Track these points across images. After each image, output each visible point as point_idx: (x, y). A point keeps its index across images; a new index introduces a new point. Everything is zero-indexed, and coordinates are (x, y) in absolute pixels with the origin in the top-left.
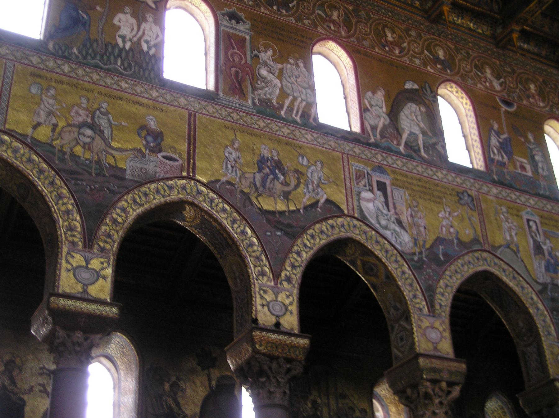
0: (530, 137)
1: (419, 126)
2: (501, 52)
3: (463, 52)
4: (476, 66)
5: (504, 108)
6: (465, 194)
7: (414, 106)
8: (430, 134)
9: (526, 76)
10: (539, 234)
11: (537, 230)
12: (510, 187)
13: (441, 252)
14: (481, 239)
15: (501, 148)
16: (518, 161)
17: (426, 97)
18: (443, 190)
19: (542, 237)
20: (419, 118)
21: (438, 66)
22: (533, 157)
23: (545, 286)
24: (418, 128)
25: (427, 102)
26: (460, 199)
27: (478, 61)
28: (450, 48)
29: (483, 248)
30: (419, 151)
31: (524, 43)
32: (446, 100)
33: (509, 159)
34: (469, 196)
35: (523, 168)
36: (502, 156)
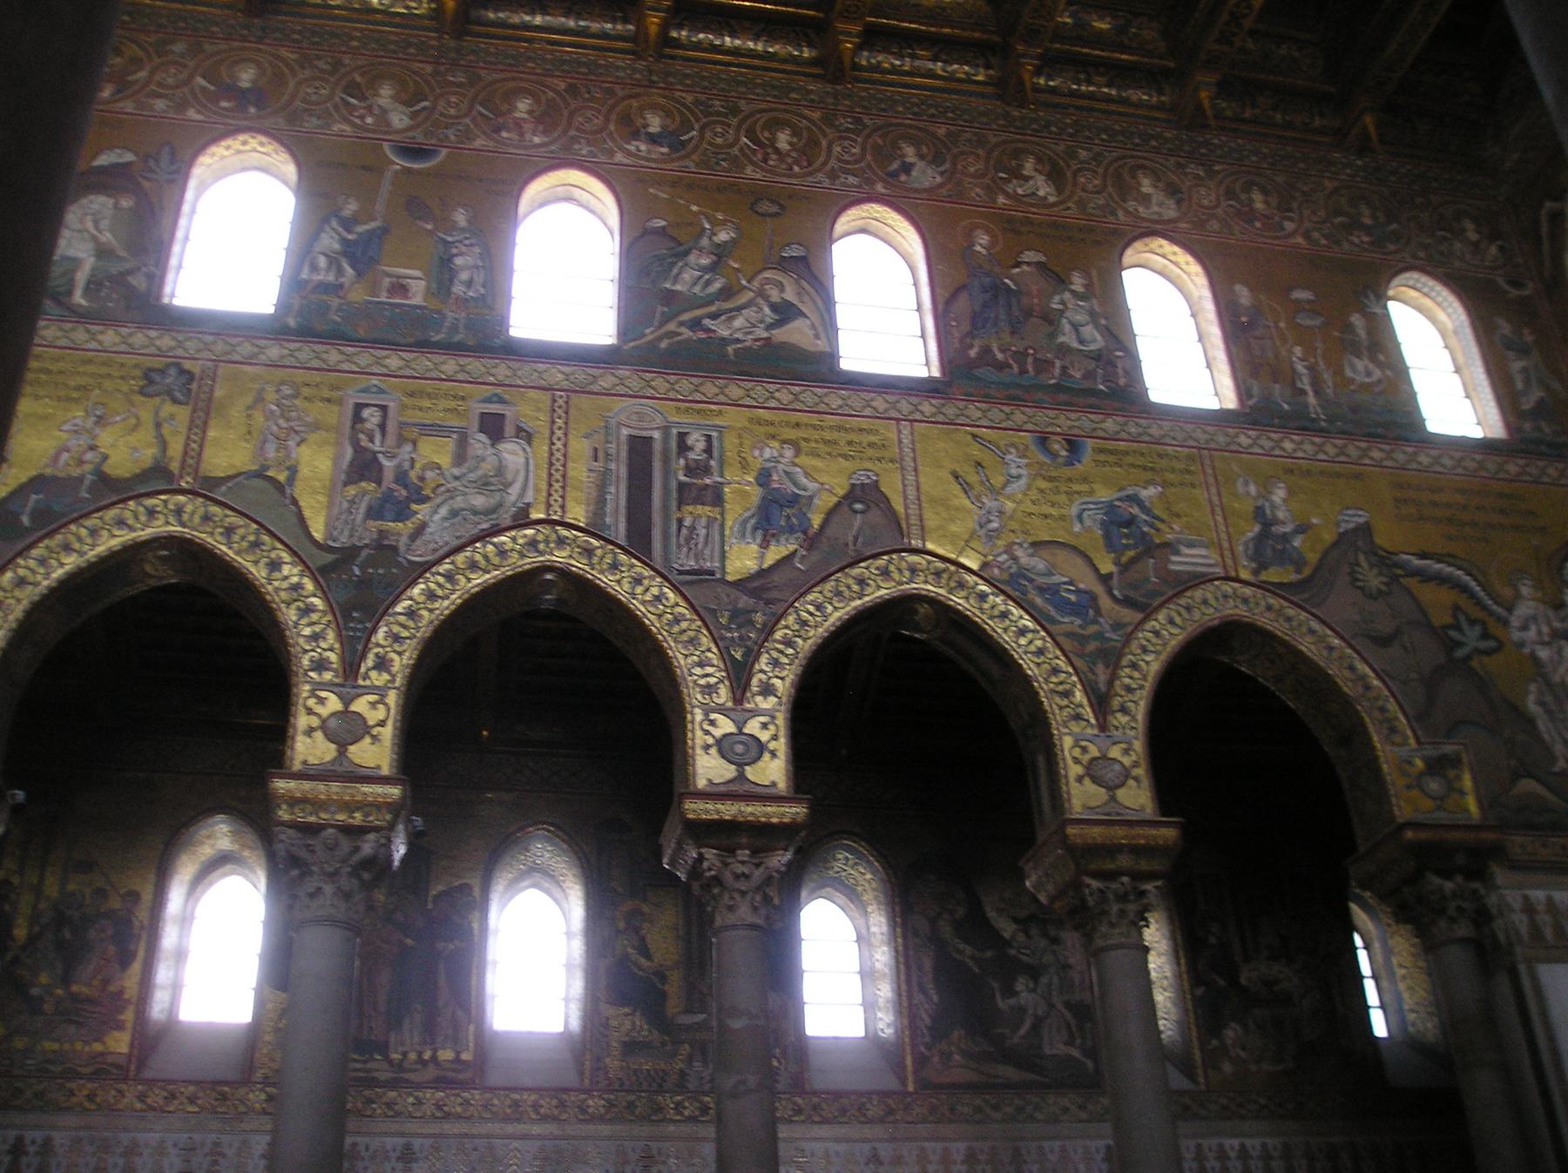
0: (461, 218)
1: (94, 239)
2: (453, 44)
3: (321, 64)
4: (353, 89)
5: (400, 163)
6: (173, 371)
7: (102, 199)
8: (123, 254)
9: (512, 84)
10: (384, 433)
11: (382, 427)
12: (335, 336)
13: (28, 509)
14: (175, 466)
15: (345, 254)
16: (390, 276)
17: (147, 175)
18: (104, 370)
19: (391, 439)
20: (104, 224)
21: (224, 104)
22: (446, 263)
23: (348, 555)
24: (90, 246)
25: (146, 184)
26: (151, 382)
27: (362, 75)
28: (283, 60)
29: (175, 486)
30: (70, 293)
31: (533, 13)
32: (276, 176)
33: (359, 274)
34: (182, 371)
35: (400, 288)
36: (340, 272)
